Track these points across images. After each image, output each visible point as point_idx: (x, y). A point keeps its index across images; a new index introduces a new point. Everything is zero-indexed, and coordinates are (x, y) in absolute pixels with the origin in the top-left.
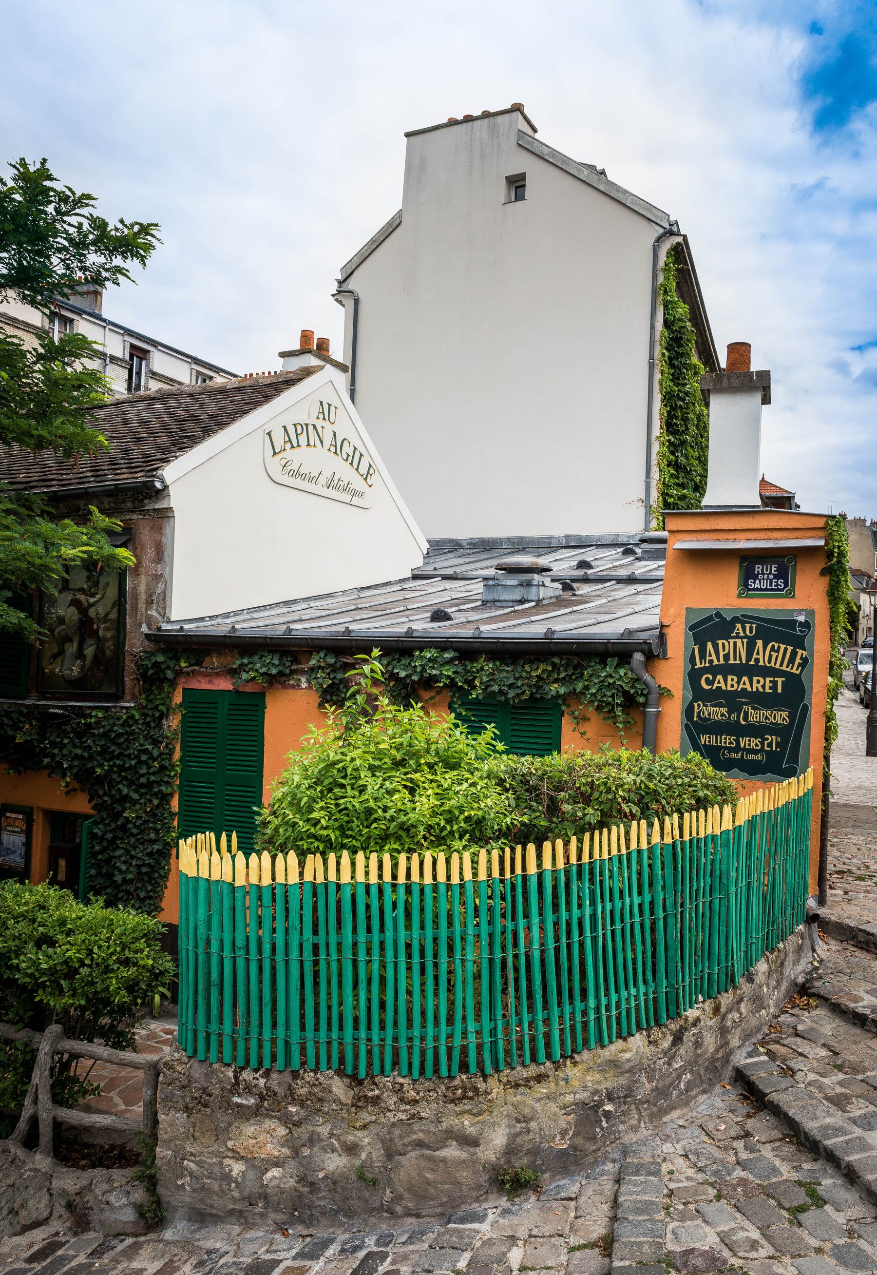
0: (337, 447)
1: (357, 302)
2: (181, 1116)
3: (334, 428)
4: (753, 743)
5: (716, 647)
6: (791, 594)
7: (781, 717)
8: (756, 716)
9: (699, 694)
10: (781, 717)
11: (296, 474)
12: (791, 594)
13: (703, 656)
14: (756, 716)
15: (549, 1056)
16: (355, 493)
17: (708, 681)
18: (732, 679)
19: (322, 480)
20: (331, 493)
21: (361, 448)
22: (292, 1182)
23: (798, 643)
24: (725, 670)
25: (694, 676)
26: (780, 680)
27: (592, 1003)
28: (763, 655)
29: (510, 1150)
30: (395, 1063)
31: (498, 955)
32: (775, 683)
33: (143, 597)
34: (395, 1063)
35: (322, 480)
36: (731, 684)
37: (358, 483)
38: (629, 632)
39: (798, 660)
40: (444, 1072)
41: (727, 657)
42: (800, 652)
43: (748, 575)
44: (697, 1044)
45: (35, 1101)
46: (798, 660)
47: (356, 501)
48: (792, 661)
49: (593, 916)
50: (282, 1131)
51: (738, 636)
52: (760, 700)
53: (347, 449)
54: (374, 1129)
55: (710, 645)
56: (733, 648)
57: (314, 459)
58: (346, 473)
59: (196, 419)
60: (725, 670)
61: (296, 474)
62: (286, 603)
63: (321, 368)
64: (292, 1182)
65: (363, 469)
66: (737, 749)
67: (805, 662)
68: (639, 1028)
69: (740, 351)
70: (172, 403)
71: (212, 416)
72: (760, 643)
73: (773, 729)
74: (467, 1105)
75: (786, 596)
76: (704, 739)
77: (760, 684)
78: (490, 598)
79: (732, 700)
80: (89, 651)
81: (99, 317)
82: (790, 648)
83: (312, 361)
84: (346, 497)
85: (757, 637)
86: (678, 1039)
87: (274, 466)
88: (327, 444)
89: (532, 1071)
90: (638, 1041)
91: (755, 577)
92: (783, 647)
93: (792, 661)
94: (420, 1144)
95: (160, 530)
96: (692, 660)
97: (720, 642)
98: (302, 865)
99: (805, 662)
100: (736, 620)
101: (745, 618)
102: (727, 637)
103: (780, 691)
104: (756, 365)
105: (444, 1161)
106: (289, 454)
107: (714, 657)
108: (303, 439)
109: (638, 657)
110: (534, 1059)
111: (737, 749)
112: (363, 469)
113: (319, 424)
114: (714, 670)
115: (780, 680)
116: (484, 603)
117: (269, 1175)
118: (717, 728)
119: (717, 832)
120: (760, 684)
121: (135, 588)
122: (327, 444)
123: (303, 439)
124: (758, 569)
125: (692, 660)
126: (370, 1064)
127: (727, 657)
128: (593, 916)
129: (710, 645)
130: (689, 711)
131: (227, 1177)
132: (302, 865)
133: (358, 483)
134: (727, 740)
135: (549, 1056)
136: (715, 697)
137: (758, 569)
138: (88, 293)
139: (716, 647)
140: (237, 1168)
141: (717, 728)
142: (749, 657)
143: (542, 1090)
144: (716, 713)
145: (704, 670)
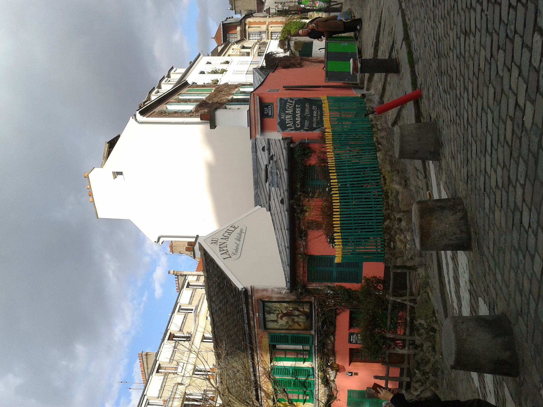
0: (227, 238)
2: (398, 260)
3: (219, 239)
4: (315, 112)
6: (272, 104)
11: (237, 250)
12: (272, 104)
13: (291, 127)
15: (379, 176)
16: (241, 231)
17: (298, 125)
19: (238, 242)
20: (242, 239)
21: (225, 230)
22: (409, 233)
23: (286, 101)
24: (294, 121)
25: (296, 129)
27: (368, 166)
28: (290, 111)
29: (400, 184)
30: (381, 210)
31: (355, 188)
32: (298, 107)
33: (279, 295)
34: (381, 210)
35: (238, 242)
36: (298, 120)
37: (238, 231)
38: (284, 148)
40: (381, 200)
43: (267, 116)
45: (405, 300)
47: (244, 231)
49: (348, 166)
50: (398, 235)
52: (303, 111)
53: (226, 234)
54: (395, 215)
56: (288, 119)
57: (231, 244)
58: (235, 235)
59: (219, 284)
60: (294, 121)
61: (237, 250)
62: (280, 253)
63: (199, 243)
64: (409, 233)
65: (233, 229)
66: (317, 117)
68: (376, 154)
70: (212, 294)
71: (218, 278)
74: (389, 194)
75: (273, 105)
78: (276, 185)
79: (303, 118)
83: (197, 247)
84: (243, 235)
86: (380, 143)
87: (234, 257)
88: (226, 241)
89: (382, 179)
90: (378, 154)
94: (398, 205)
95: (257, 290)
98: (336, 232)
99: (291, 99)
100: (280, 119)
101: (280, 116)
105: (402, 199)
106: (230, 253)
108: (225, 249)
109: (291, 145)
110: (380, 179)
111: (317, 117)
112: (233, 229)
113: (219, 244)
114: (294, 124)
116: (278, 187)
119: (331, 134)
120: (298, 111)
121: (276, 298)
122: (226, 241)
123: (225, 249)
124: (266, 113)
125: (292, 130)
126: (381, 216)
128: (348, 166)
130: (307, 130)
132: (336, 232)
133: (238, 231)
134: (315, 119)
135: (379, 176)
136: (302, 123)
140: (408, 246)
141: (311, 123)
142: (290, 115)
143: (387, 177)
144: (307, 123)
145: (295, 126)
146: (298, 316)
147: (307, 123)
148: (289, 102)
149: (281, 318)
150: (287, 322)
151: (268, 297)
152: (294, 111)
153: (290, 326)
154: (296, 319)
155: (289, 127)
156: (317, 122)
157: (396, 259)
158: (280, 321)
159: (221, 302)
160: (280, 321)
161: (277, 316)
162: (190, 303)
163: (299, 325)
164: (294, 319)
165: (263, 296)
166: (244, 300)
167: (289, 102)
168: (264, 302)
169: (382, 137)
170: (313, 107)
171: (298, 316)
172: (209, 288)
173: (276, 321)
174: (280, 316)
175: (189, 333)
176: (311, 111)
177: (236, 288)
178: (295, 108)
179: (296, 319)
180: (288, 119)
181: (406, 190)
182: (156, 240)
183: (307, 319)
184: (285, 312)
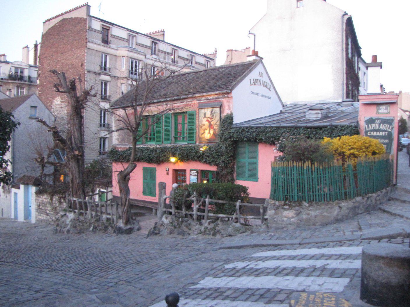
1: (255, 36)
5: (371, 126)
7: (387, 141)
10: (387, 141)
17: (370, 134)
22: (296, 221)
23: (391, 124)
24: (374, 131)
26: (386, 133)
28: (382, 127)
36: (375, 134)
39: (390, 128)
41: (374, 128)
42: (391, 126)
44: (371, 201)
46: (390, 128)
48: (389, 128)
50: (294, 212)
51: (376, 123)
55: (370, 125)
56: (376, 126)
60: (374, 131)
64: (296, 221)
67: (392, 128)
69: (375, 58)
72: (381, 124)
80: (212, 132)
81: (163, 41)
82: (389, 125)
83: (254, 58)
85: (381, 123)
91: (380, 109)
92: (387, 125)
93: (389, 128)
96: (366, 129)
97: (372, 124)
101: (378, 119)
103: (386, 135)
104: (379, 61)
107: (371, 128)
114: (371, 131)
115: (386, 133)
117: (292, 220)
120: (382, 134)
127: (374, 128)
129: (370, 125)
131: (283, 221)
137: (381, 107)
138: (161, 35)
139: (371, 126)
140: (285, 219)
146: (209, 133)
148: (390, 127)
149: (207, 121)
150: (204, 125)
151: (224, 111)
152: (383, 131)
153: (201, 127)
154: (207, 132)
157: (274, 210)
158: (206, 119)
159: (216, 76)
160: (206, 119)
161: (209, 117)
162: (196, 63)
163: (202, 134)
164: (207, 129)
165: (225, 106)
166: (221, 92)
167: (390, 127)
168: (220, 107)
169: (371, 201)
171: (209, 133)
172: (224, 68)
173: (205, 117)
174: (209, 119)
175: (177, 63)
178: (385, 131)
179: (207, 132)
180: (376, 126)
181: (332, 219)
182: (251, 32)
183: (207, 140)
184: (212, 123)
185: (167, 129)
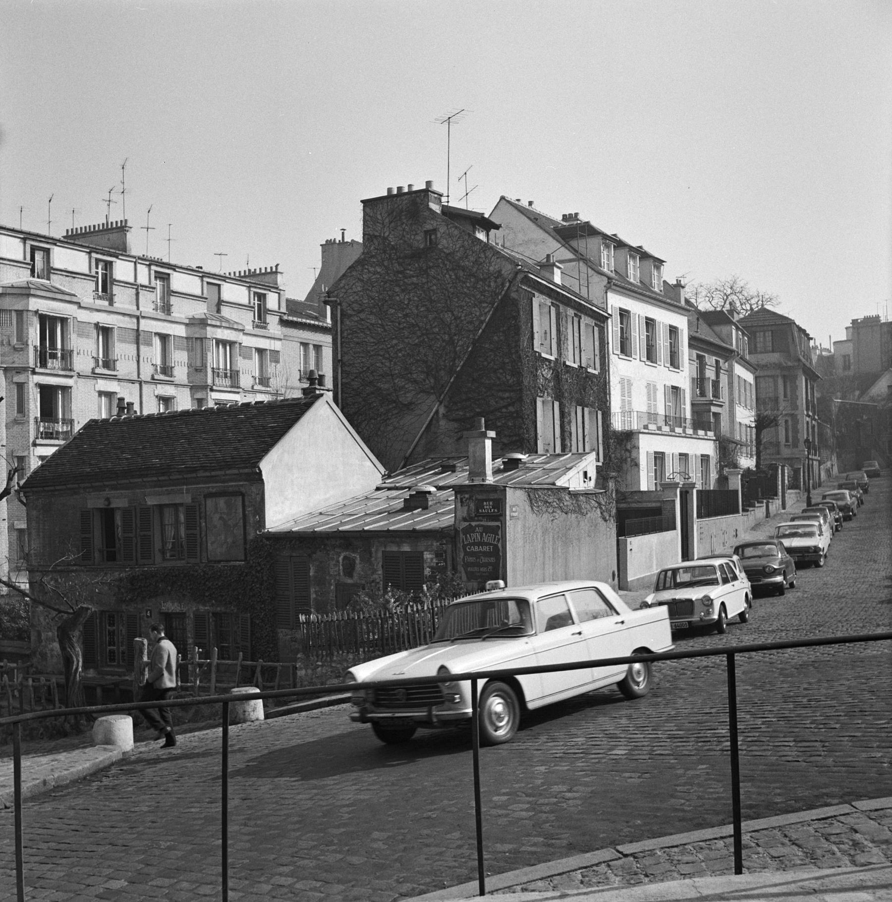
7: (492, 560)
8: (484, 560)
9: (466, 553)
10: (492, 560)
14: (484, 560)
18: (476, 547)
52: (485, 554)
56: (476, 536)
60: (474, 544)
73: (490, 564)
76: (469, 569)
77: (486, 549)
100: (476, 526)
101: (478, 526)
102: (473, 532)
118: (472, 565)
120: (486, 549)
134: (476, 569)
136: (473, 554)
144: (471, 559)
147: (471, 559)
155: (466, 537)
156: (473, 572)
170: (490, 567)
176: (486, 565)
177: (260, 458)
180: (476, 536)
185: (144, 536)
